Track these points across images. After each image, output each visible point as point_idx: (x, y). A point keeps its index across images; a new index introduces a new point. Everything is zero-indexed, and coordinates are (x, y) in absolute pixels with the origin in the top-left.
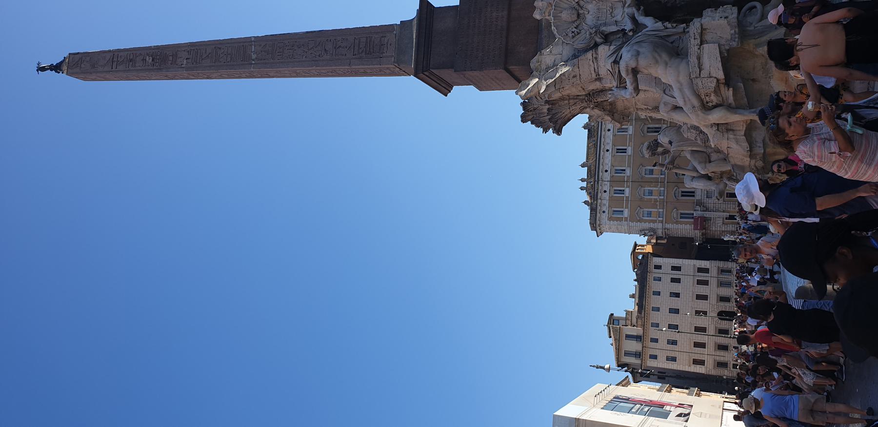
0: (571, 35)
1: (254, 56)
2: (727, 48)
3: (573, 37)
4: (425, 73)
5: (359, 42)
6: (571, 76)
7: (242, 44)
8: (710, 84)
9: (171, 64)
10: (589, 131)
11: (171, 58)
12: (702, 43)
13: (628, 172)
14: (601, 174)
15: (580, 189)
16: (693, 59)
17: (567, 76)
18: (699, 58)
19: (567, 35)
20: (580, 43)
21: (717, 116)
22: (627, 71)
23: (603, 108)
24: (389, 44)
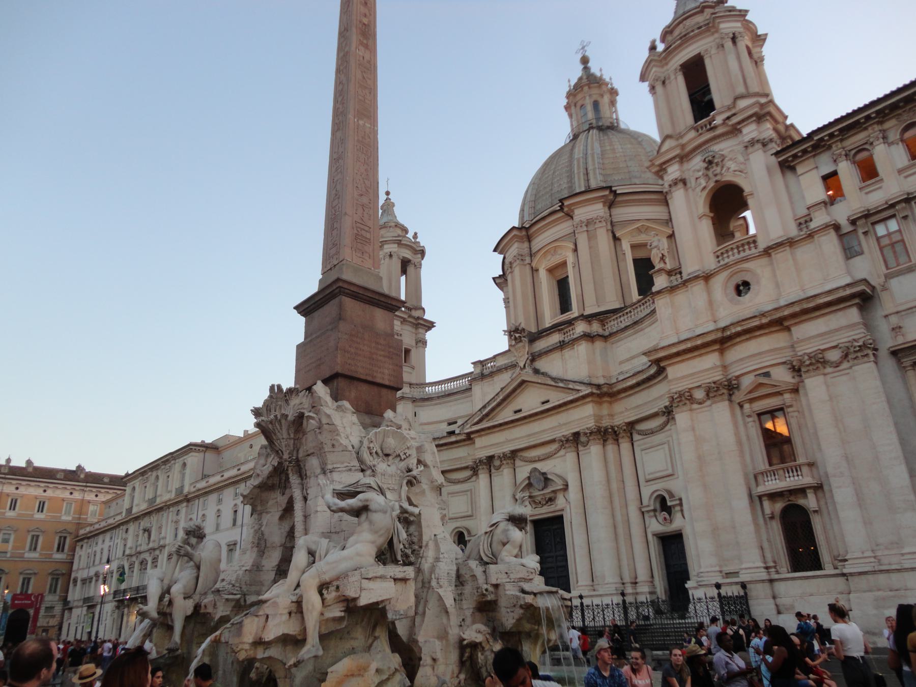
0: (372, 445)
1: (361, 122)
2: (387, 608)
3: (369, 448)
4: (338, 289)
5: (367, 231)
6: (335, 443)
7: (372, 115)
8: (353, 590)
9: (360, 40)
10: (74, 471)
11: (365, 42)
12: (395, 580)
13: (11, 514)
14: (14, 482)
15: (7, 458)
16: (381, 570)
17: (336, 437)
18: (382, 577)
19: (372, 442)
20: (366, 456)
21: (313, 600)
22: (367, 500)
23: (271, 476)
24: (361, 259)
